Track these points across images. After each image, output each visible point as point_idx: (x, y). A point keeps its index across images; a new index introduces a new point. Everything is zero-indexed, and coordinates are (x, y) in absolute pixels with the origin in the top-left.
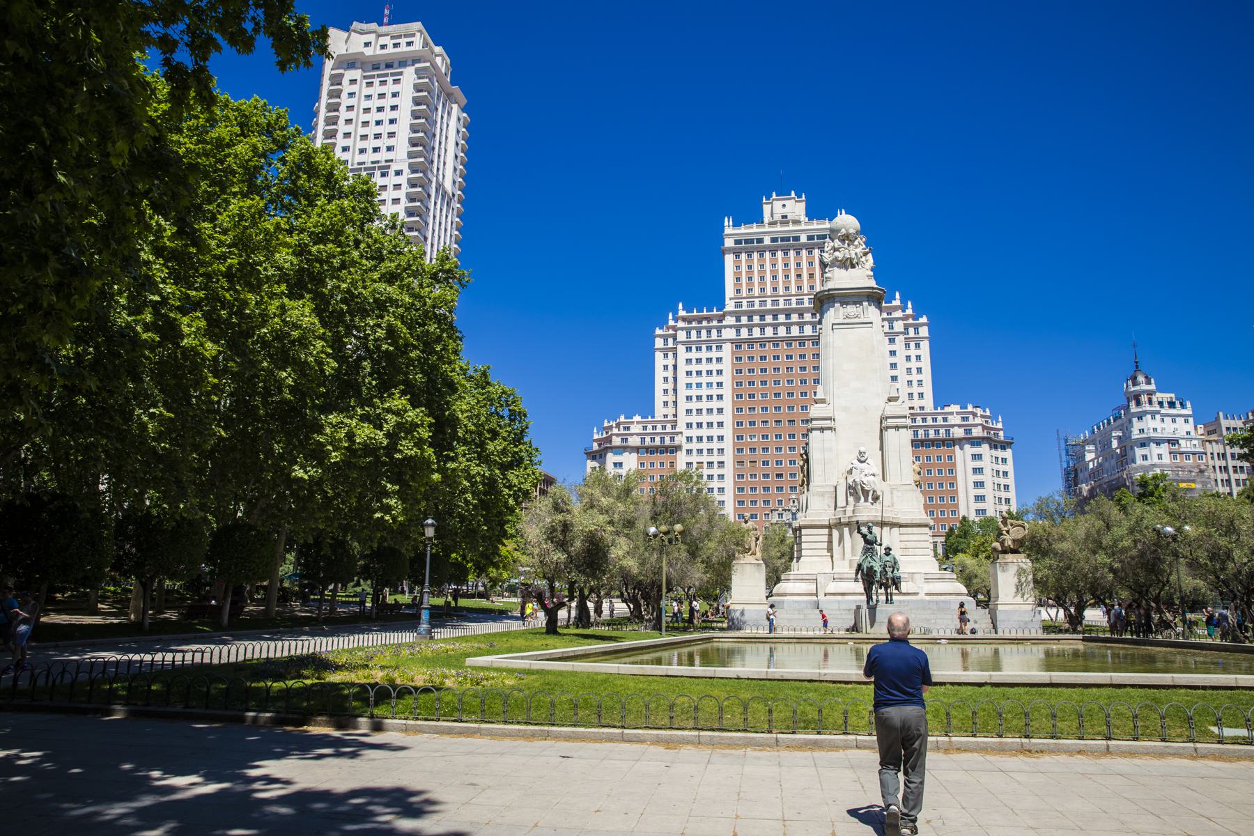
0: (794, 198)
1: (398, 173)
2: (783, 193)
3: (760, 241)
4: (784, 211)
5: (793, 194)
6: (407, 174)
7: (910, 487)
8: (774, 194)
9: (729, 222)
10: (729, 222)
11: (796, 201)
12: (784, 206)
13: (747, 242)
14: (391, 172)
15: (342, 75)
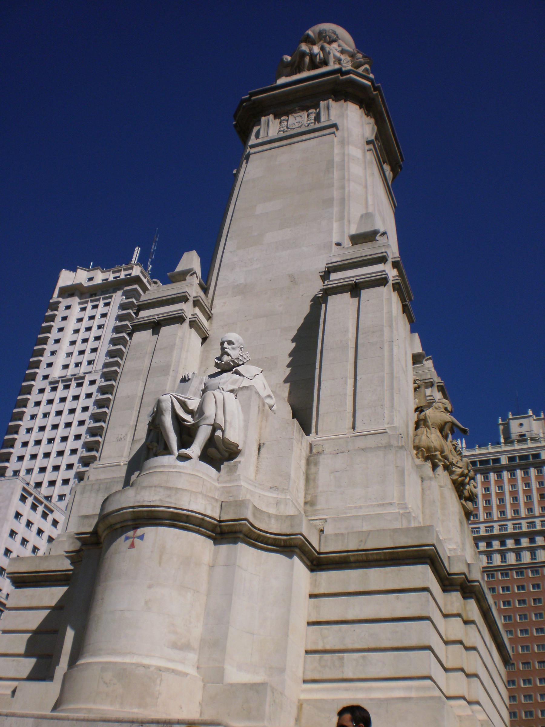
0: (531, 416)
1: (92, 382)
2: (520, 412)
3: (497, 461)
4: (522, 430)
5: (530, 413)
6: (101, 382)
7: (371, 442)
8: (510, 413)
9: (462, 443)
10: (462, 443)
11: (534, 420)
12: (521, 425)
13: (482, 462)
14: (86, 382)
15: (59, 302)
